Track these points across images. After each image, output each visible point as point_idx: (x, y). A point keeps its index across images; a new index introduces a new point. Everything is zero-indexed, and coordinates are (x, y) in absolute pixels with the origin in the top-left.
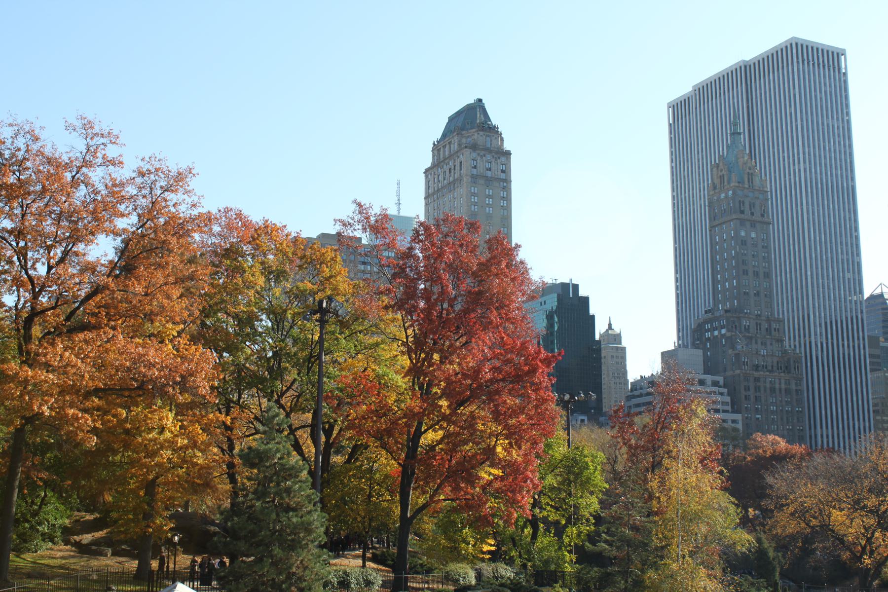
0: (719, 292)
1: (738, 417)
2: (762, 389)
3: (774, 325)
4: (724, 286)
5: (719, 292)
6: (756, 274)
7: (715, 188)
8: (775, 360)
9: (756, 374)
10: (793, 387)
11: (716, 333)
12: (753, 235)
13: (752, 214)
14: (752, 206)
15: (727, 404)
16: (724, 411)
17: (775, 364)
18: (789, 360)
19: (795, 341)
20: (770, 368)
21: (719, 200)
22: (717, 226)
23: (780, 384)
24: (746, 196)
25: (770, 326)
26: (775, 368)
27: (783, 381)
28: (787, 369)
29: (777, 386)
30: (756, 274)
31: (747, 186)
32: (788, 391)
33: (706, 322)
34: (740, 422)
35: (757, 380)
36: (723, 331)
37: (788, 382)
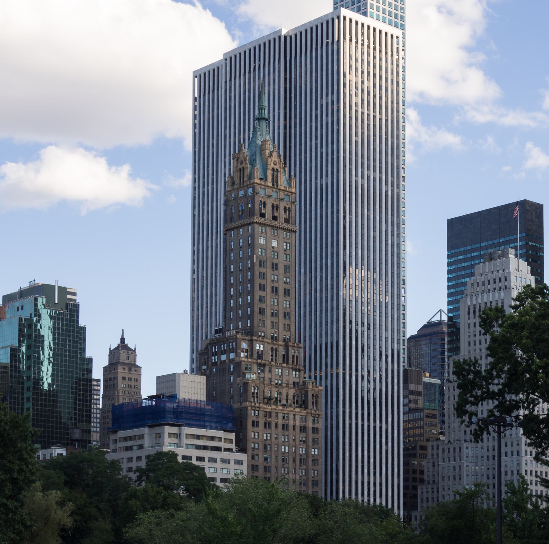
0: (231, 309)
1: (243, 457)
2: (273, 426)
4: (237, 302)
5: (231, 309)
6: (275, 290)
7: (233, 183)
9: (267, 408)
10: (310, 425)
11: (224, 357)
12: (274, 244)
13: (275, 218)
14: (275, 207)
15: (231, 441)
16: (226, 450)
17: (291, 397)
19: (321, 371)
20: (284, 402)
21: (237, 198)
22: (232, 229)
23: (295, 419)
24: (270, 196)
25: (287, 352)
27: (298, 417)
28: (304, 405)
29: (291, 423)
30: (275, 290)
31: (270, 184)
32: (303, 429)
33: (213, 343)
34: (245, 464)
35: (268, 414)
36: (232, 356)
37: (304, 419)
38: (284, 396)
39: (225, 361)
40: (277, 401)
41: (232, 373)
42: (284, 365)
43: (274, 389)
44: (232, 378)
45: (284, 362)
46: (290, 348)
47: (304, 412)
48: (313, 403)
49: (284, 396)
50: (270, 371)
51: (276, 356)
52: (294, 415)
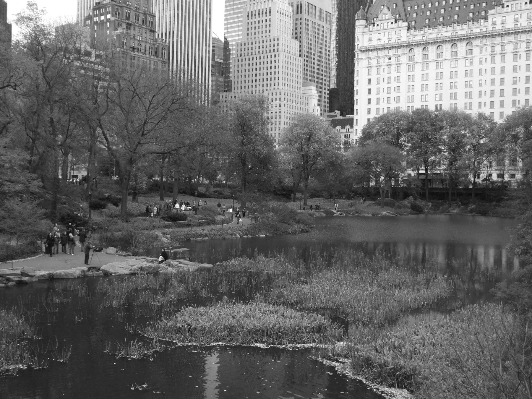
3: (149, 19)
8: (148, 46)
11: (102, 18)
17: (147, 49)
18: (158, 46)
20: (143, 51)
23: (150, 64)
26: (147, 52)
27: (152, 62)
35: (133, 58)
38: (143, 48)
39: (103, 20)
40: (139, 50)
41: (108, 28)
42: (144, 26)
43: (137, 42)
44: (108, 32)
45: (143, 24)
46: (148, 16)
47: (156, 59)
48: (162, 54)
49: (143, 48)
50: (134, 30)
51: (138, 20)
52: (150, 61)
